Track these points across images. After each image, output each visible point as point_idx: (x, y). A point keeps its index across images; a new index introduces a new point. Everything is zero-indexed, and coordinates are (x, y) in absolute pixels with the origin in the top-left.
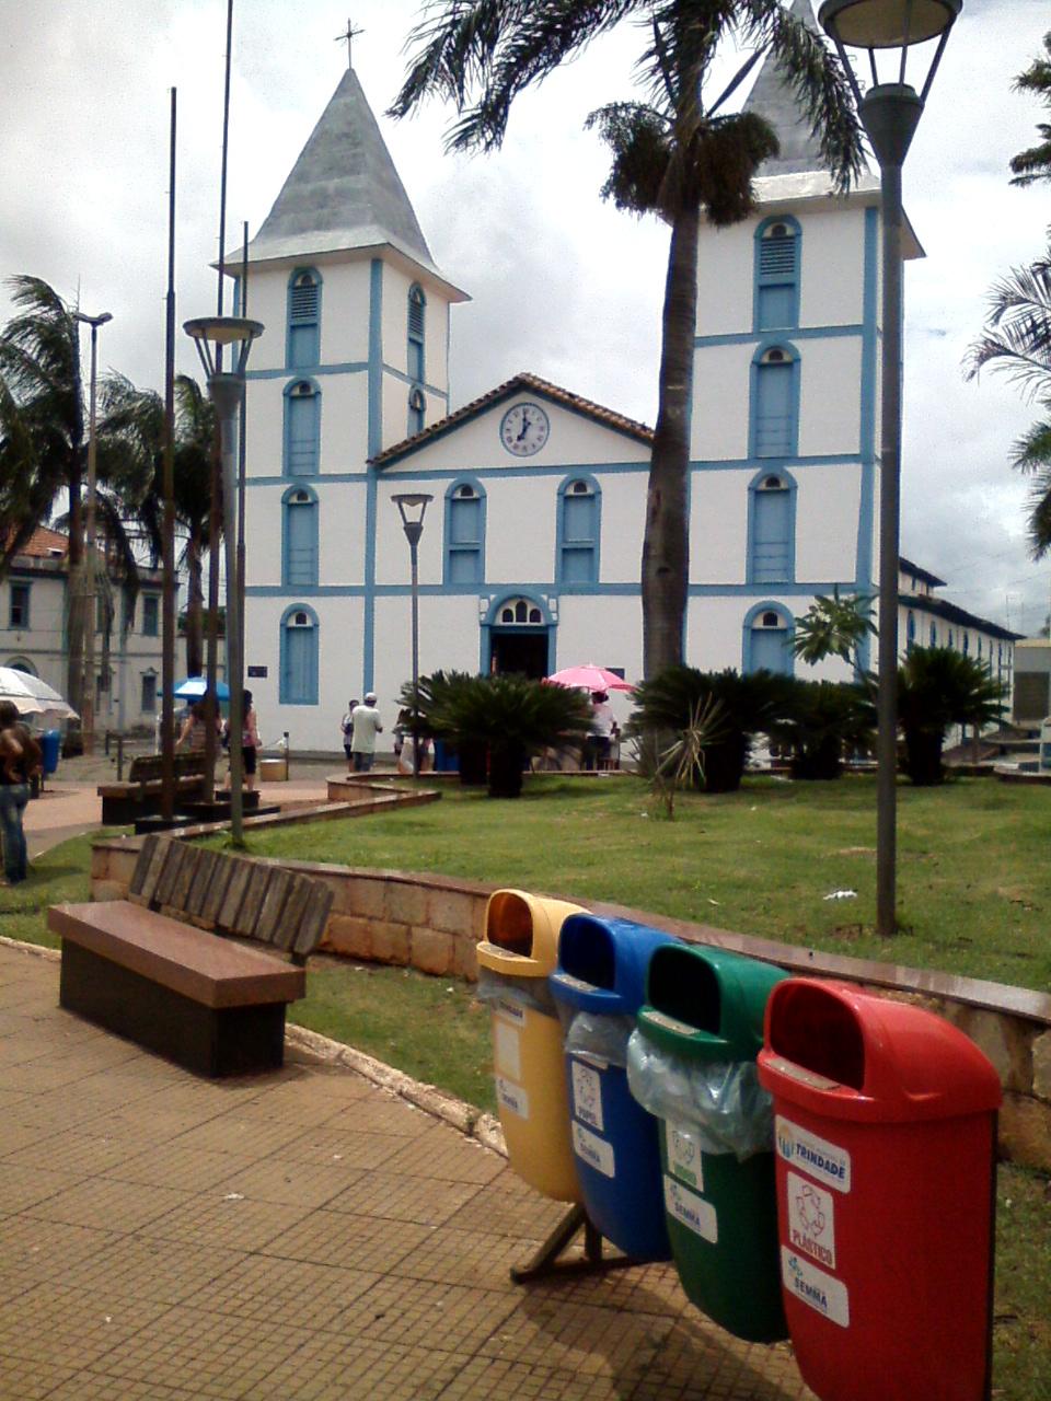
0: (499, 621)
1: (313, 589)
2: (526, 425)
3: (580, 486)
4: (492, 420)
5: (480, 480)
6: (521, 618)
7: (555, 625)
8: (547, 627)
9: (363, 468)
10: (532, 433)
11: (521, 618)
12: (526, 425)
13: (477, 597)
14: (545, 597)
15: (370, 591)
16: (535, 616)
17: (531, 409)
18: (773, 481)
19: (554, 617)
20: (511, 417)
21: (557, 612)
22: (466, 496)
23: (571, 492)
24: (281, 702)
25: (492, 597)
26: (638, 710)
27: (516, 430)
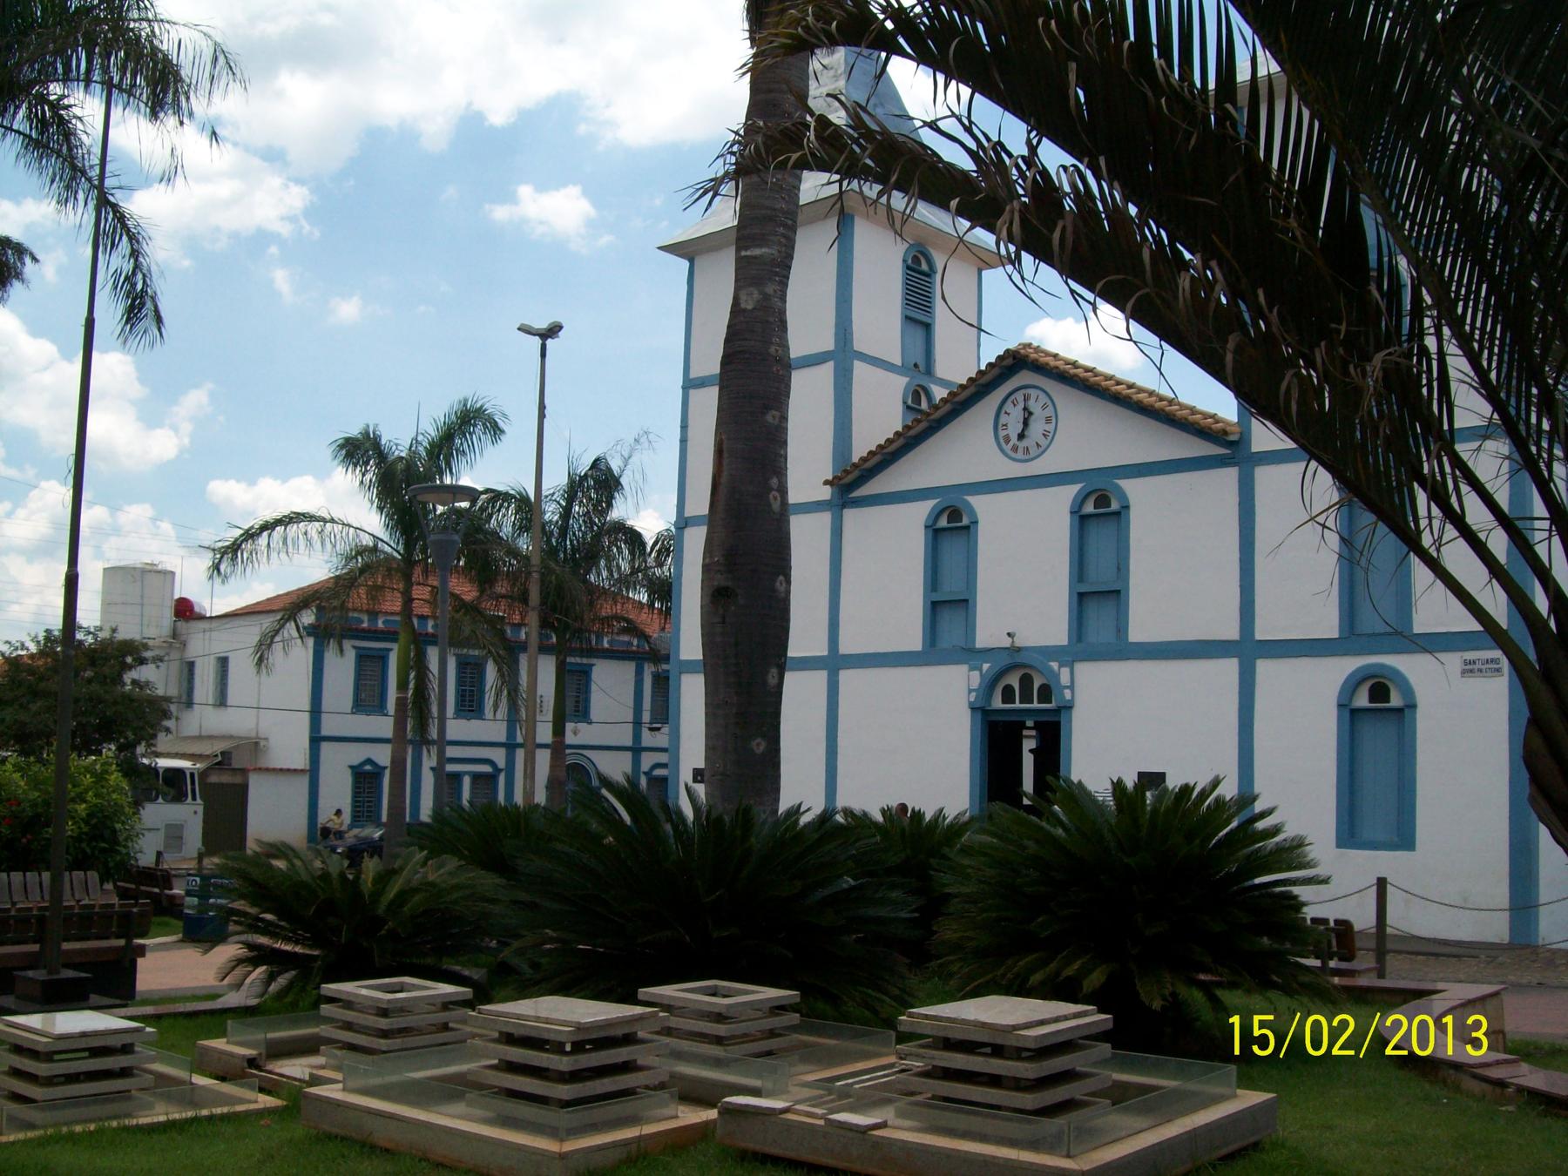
0: (997, 703)
2: (1028, 414)
3: (1102, 500)
5: (970, 499)
6: (1026, 698)
7: (1069, 707)
8: (1058, 711)
9: (826, 493)
10: (1037, 428)
11: (1026, 698)
12: (1028, 414)
13: (965, 668)
14: (1055, 665)
16: (1046, 693)
19: (1067, 694)
20: (1008, 407)
21: (1072, 687)
22: (951, 526)
23: (1089, 508)
25: (986, 666)
26: (928, 817)
27: (1014, 429)
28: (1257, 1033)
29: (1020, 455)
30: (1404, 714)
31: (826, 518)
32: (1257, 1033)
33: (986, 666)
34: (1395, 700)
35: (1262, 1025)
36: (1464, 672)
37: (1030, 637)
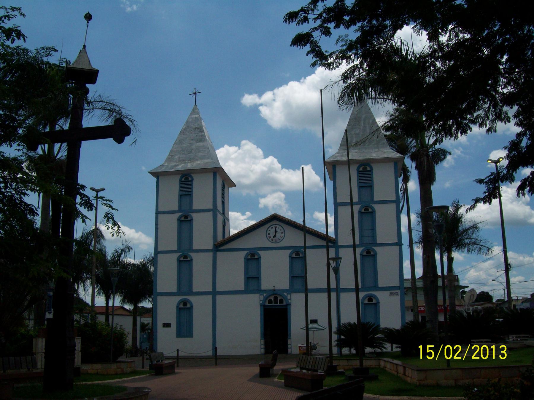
0: (267, 304)
1: (190, 292)
2: (276, 231)
4: (263, 229)
6: (276, 302)
7: (290, 304)
10: (278, 235)
11: (276, 302)
12: (276, 231)
14: (286, 294)
15: (214, 293)
16: (281, 301)
17: (278, 226)
18: (368, 252)
20: (270, 229)
21: (290, 300)
22: (253, 258)
23: (294, 256)
24: (177, 337)
25: (265, 294)
28: (428, 351)
29: (274, 241)
30: (377, 305)
31: (211, 254)
32: (428, 351)
33: (265, 294)
34: (374, 301)
35: (430, 348)
36: (390, 295)
37: (279, 287)
